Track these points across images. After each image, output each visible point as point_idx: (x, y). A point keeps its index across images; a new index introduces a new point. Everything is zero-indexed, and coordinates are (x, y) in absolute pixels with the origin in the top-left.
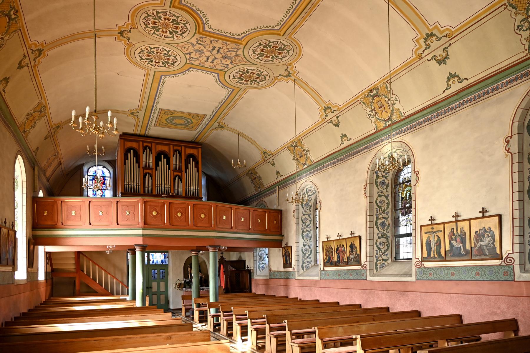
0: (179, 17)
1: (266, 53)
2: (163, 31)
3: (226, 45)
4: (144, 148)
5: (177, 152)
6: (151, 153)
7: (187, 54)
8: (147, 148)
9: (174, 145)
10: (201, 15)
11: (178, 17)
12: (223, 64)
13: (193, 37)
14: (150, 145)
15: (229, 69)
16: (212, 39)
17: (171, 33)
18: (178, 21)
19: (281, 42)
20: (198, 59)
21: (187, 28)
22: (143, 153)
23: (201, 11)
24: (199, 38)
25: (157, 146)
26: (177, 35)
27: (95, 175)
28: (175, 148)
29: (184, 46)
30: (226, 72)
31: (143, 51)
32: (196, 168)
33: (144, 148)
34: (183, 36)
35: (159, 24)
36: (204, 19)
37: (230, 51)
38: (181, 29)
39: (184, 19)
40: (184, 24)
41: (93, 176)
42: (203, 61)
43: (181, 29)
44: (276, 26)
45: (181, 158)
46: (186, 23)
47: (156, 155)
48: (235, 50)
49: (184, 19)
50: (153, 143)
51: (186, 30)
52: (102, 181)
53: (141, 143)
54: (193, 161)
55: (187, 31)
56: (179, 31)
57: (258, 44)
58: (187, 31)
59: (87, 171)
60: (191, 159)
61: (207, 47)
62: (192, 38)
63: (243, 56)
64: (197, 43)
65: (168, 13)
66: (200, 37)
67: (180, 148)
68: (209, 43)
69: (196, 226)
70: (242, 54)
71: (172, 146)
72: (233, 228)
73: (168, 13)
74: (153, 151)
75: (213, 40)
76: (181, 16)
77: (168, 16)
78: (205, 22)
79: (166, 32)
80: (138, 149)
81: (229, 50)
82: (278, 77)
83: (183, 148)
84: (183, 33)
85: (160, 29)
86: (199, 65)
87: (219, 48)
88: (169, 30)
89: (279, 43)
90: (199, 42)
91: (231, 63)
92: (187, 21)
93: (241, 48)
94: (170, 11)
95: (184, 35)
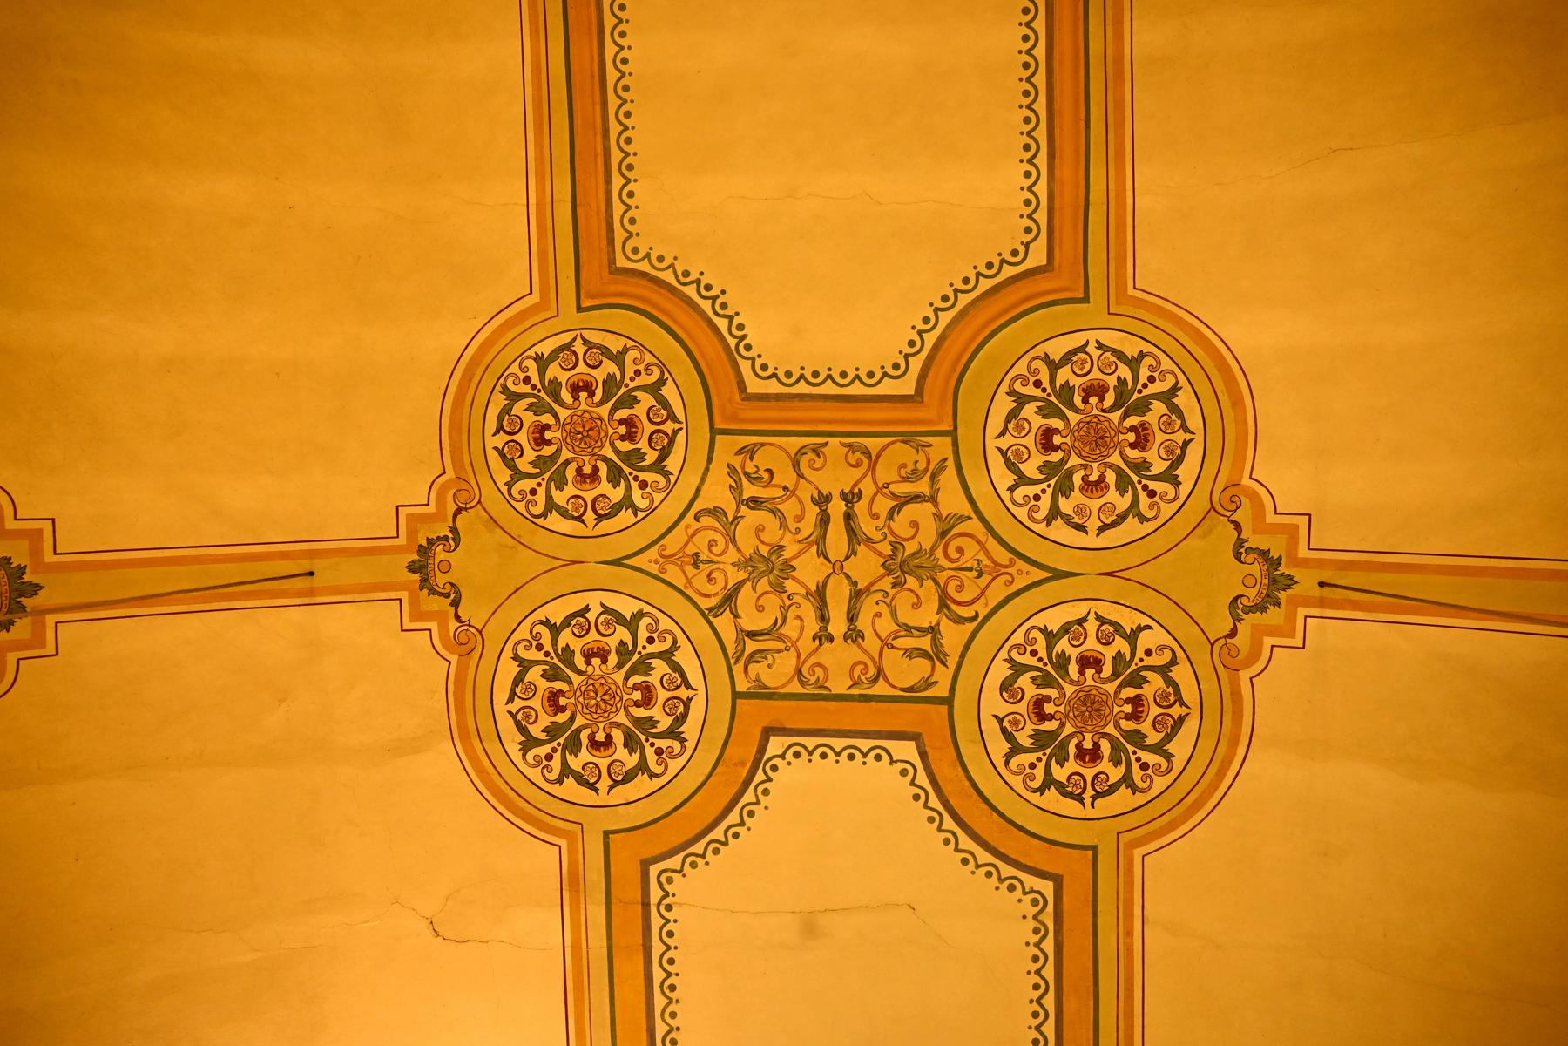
0: (626, 350)
1: (1074, 460)
2: (579, 471)
3: (866, 462)
7: (716, 611)
10: (706, 306)
11: (618, 358)
12: (908, 629)
13: (710, 460)
15: (952, 662)
16: (796, 442)
17: (615, 477)
18: (627, 380)
19: (1100, 346)
20: (780, 638)
21: (672, 417)
23: (698, 282)
24: (737, 462)
26: (643, 476)
29: (690, 550)
30: (948, 701)
31: (525, 665)
34: (667, 474)
35: (558, 434)
36: (722, 324)
37: (902, 502)
38: (649, 428)
39: (649, 358)
40: (654, 389)
42: (807, 645)
43: (649, 428)
44: (1027, 245)
46: (662, 381)
48: (923, 487)
49: (649, 358)
51: (669, 427)
55: (675, 432)
56: (643, 445)
57: (1004, 404)
58: (675, 432)
61: (789, 508)
62: (707, 469)
63: (974, 526)
64: (740, 501)
65: (579, 348)
66: (738, 453)
68: (789, 478)
70: (966, 509)
73: (579, 348)
75: (801, 452)
76: (631, 343)
77: (581, 367)
78: (732, 342)
79: (594, 476)
81: (894, 496)
82: (1233, 633)
84: (664, 454)
85: (567, 463)
86: (795, 687)
87: (843, 496)
88: (605, 459)
89: (1091, 349)
90: (750, 490)
91: (944, 602)
92: (662, 367)
93: (941, 467)
94: (586, 334)
95: (673, 463)
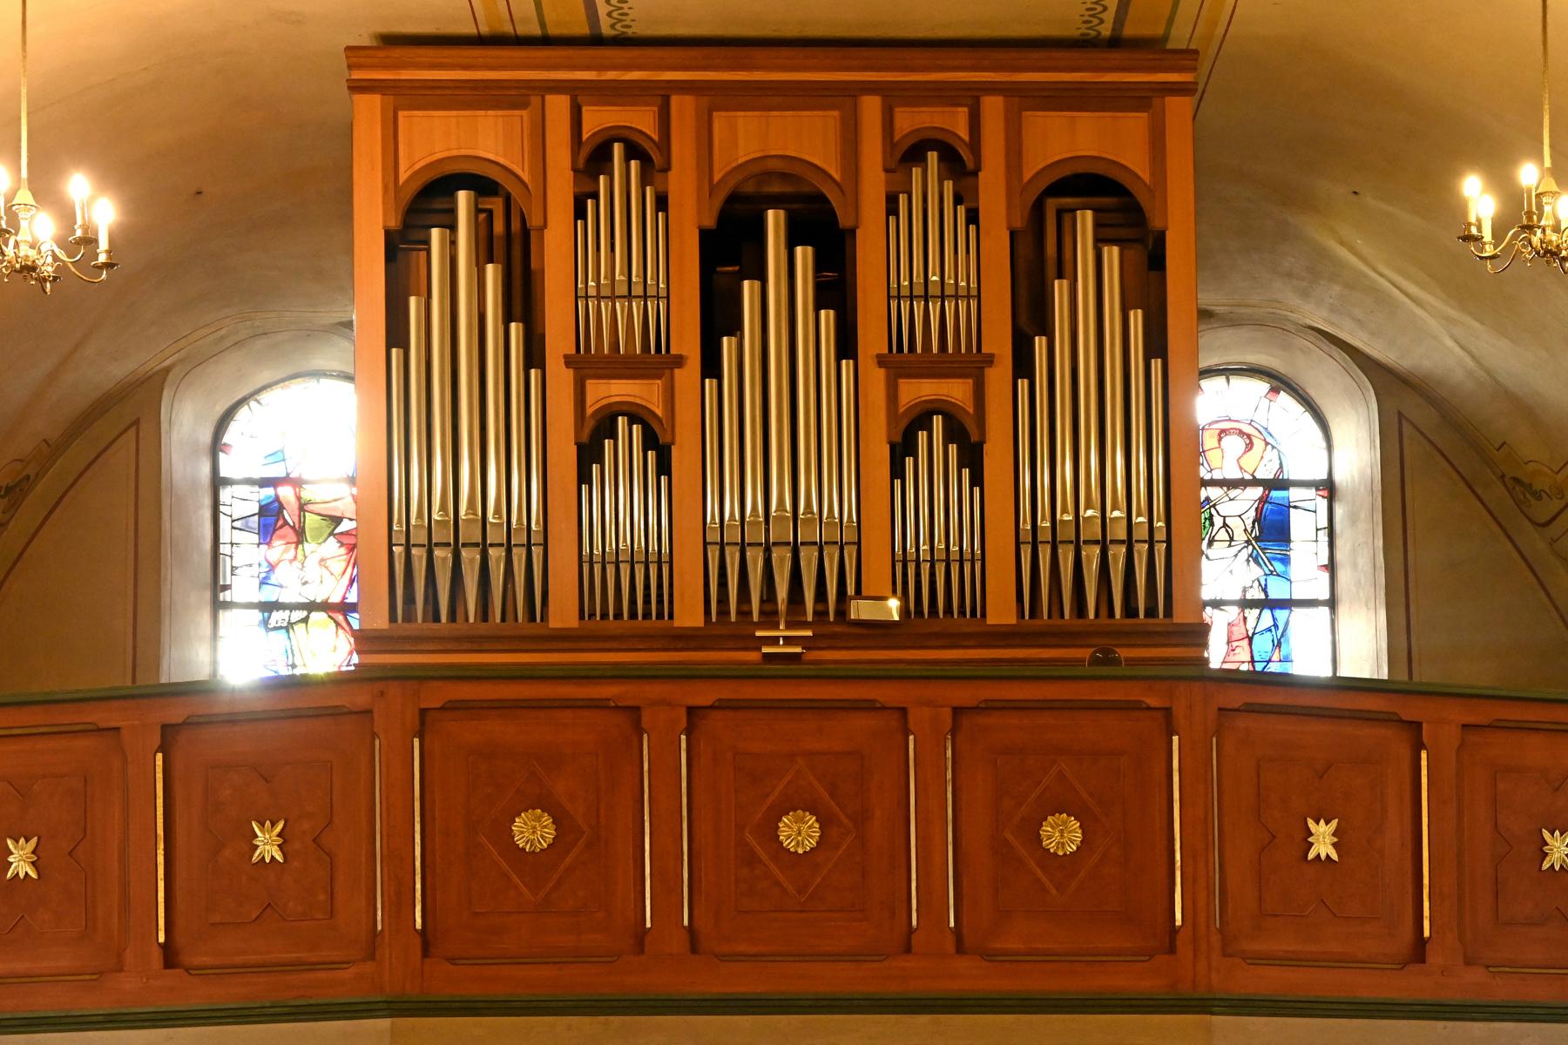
4: (594, 161)
5: (933, 157)
6: (662, 203)
8: (617, 149)
9: (893, 96)
14: (642, 120)
22: (580, 213)
25: (720, 120)
27: (276, 471)
28: (910, 121)
33: (594, 161)
41: (264, 483)
45: (973, 217)
47: (710, 222)
50: (675, 100)
52: (346, 526)
53: (558, 106)
54: (1100, 241)
59: (206, 436)
60: (1086, 221)
67: (957, 122)
69: (988, 955)
71: (871, 106)
72: (1434, 958)
74: (682, 181)
80: (526, 177)
83: (993, 106)
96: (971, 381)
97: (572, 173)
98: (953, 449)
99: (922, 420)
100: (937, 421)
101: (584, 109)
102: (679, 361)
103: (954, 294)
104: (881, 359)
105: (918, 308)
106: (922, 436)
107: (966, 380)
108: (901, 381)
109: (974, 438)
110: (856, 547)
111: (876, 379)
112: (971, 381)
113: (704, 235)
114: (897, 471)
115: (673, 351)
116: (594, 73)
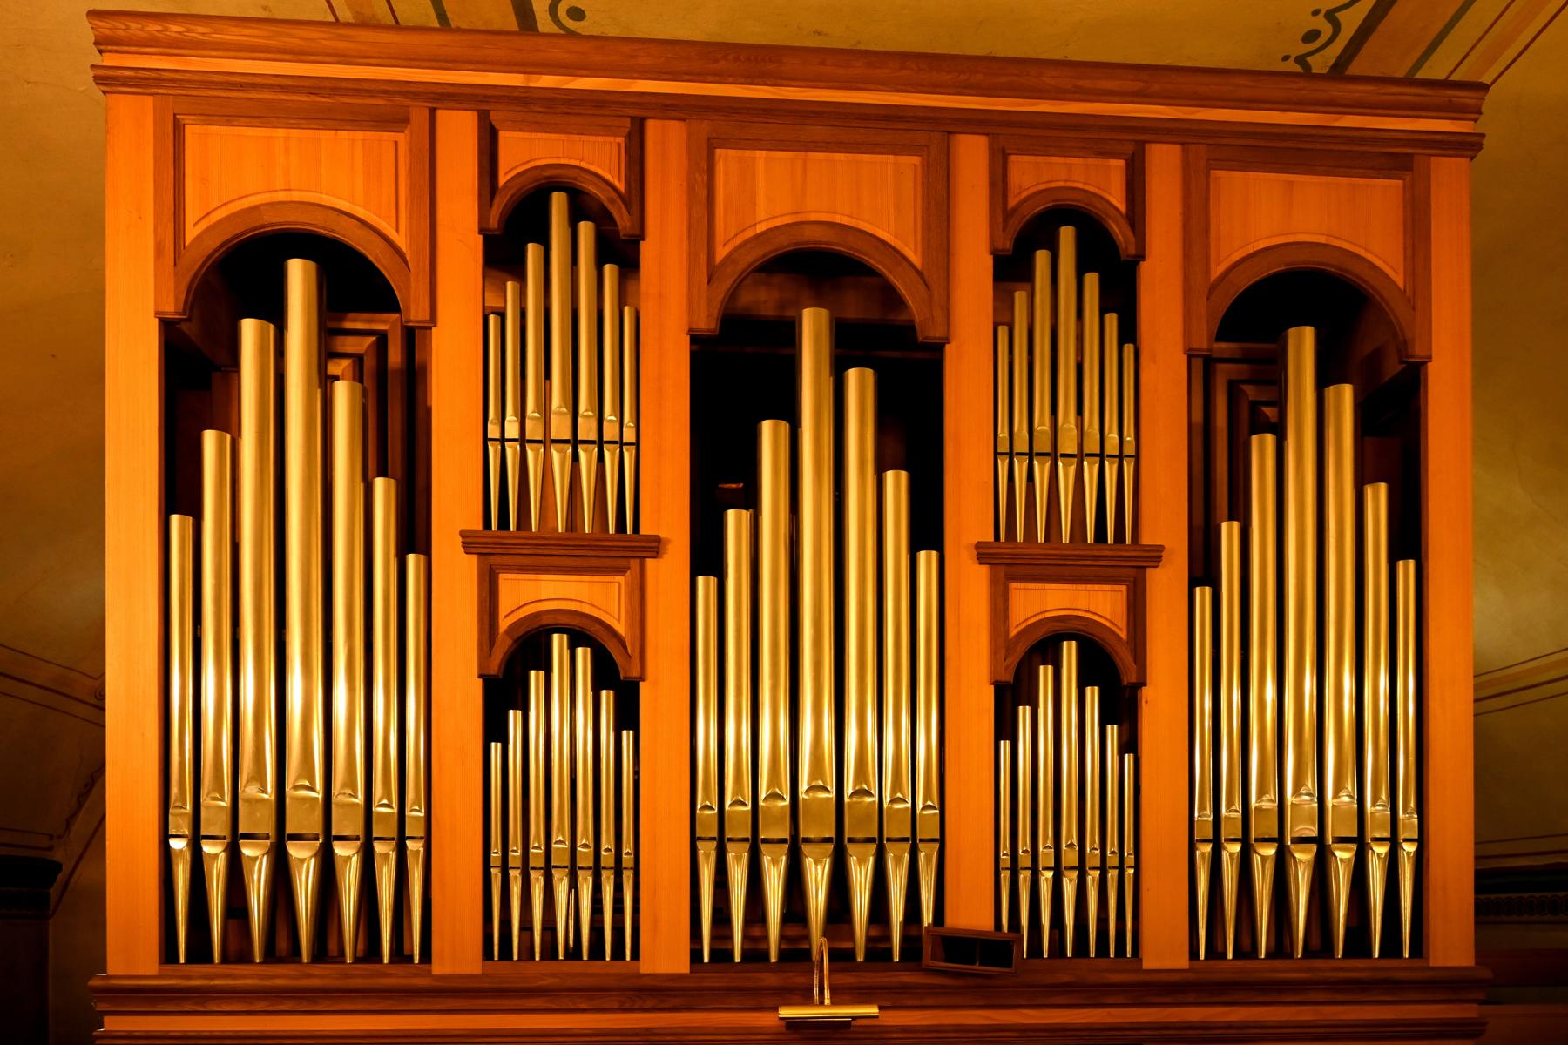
8: (558, 202)
32: (1378, 497)
47: (707, 323)
96: (1124, 588)
97: (480, 237)
98: (1093, 694)
99: (1045, 648)
100: (1069, 651)
101: (502, 135)
102: (654, 547)
103: (1117, 453)
104: (981, 551)
105: (1041, 471)
106: (1045, 673)
107: (1117, 587)
108: (1013, 585)
109: (1129, 677)
110: (937, 845)
111: (972, 582)
112: (1124, 588)
113: (698, 342)
114: (1005, 728)
115: (645, 530)
116: (521, 76)
